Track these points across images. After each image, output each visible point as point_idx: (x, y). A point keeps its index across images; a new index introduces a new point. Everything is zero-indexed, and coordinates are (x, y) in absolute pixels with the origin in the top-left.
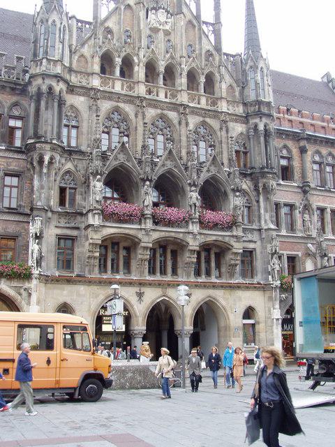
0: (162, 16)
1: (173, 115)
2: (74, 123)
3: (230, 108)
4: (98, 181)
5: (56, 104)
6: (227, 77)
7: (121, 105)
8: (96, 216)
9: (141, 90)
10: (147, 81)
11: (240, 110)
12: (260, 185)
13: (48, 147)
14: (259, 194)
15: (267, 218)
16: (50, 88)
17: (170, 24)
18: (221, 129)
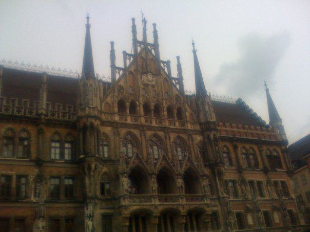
0: (150, 77)
1: (161, 134)
2: (105, 143)
3: (192, 126)
4: (125, 177)
5: (96, 133)
6: (188, 109)
7: (132, 130)
8: (126, 199)
9: (143, 120)
10: (144, 115)
11: (198, 127)
12: (216, 170)
13: (93, 159)
14: (215, 176)
15: (222, 190)
16: (92, 124)
17: (154, 81)
18: (189, 140)
